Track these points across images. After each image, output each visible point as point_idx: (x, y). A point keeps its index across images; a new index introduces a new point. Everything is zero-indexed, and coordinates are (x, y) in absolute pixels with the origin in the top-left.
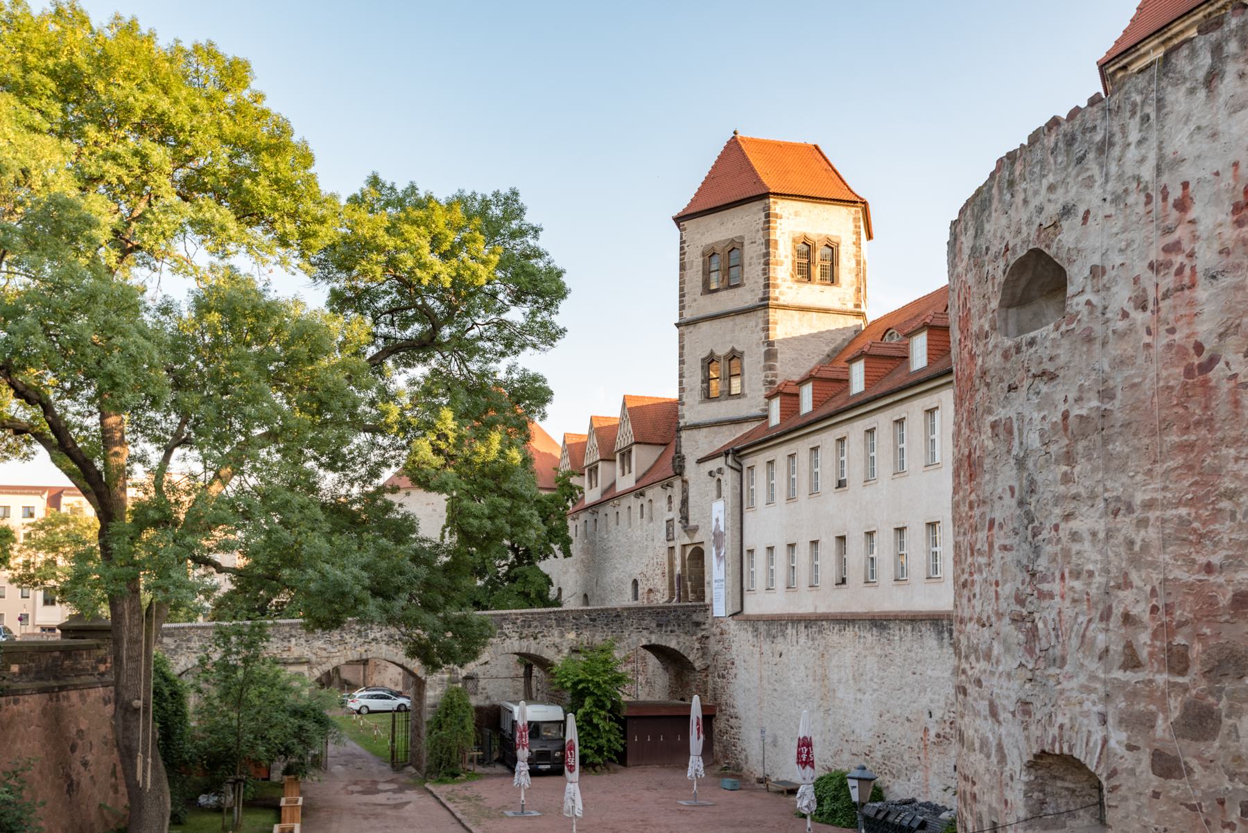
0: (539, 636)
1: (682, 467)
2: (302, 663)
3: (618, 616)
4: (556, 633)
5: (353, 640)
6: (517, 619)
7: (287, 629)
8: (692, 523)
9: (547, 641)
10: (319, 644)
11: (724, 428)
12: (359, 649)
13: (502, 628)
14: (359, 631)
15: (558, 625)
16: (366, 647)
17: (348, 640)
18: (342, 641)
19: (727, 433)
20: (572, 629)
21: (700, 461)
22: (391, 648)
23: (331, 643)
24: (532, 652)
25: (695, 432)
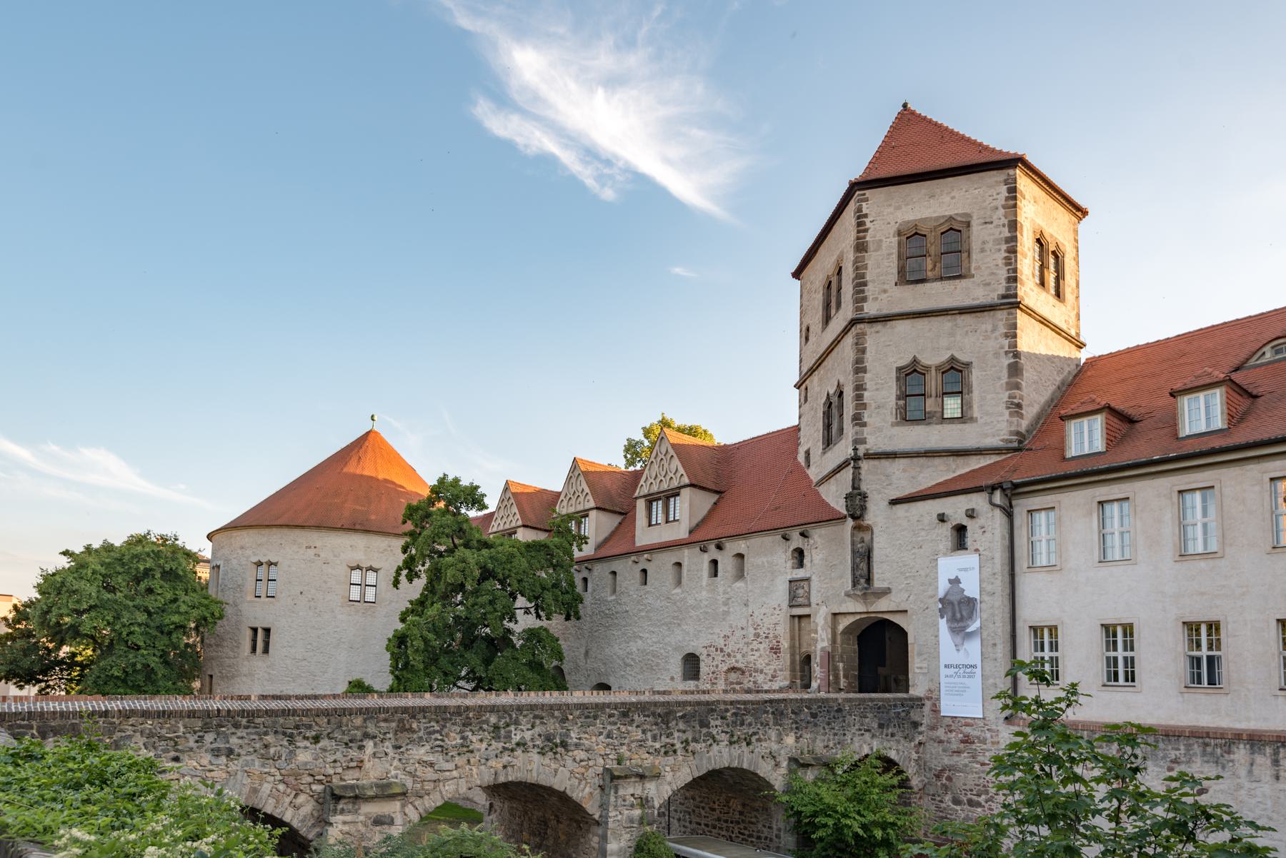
0: (753, 739)
1: (864, 508)
2: (392, 797)
3: (839, 710)
4: (773, 734)
5: (484, 745)
6: (727, 710)
7: (358, 721)
8: (878, 583)
9: (761, 748)
10: (420, 752)
11: (937, 461)
12: (492, 763)
13: (707, 726)
14: (496, 728)
15: (776, 724)
16: (506, 758)
17: (476, 745)
18: (465, 748)
19: (942, 468)
20: (792, 729)
21: (894, 502)
22: (547, 761)
23: (444, 750)
24: (745, 766)
25: (885, 463)
